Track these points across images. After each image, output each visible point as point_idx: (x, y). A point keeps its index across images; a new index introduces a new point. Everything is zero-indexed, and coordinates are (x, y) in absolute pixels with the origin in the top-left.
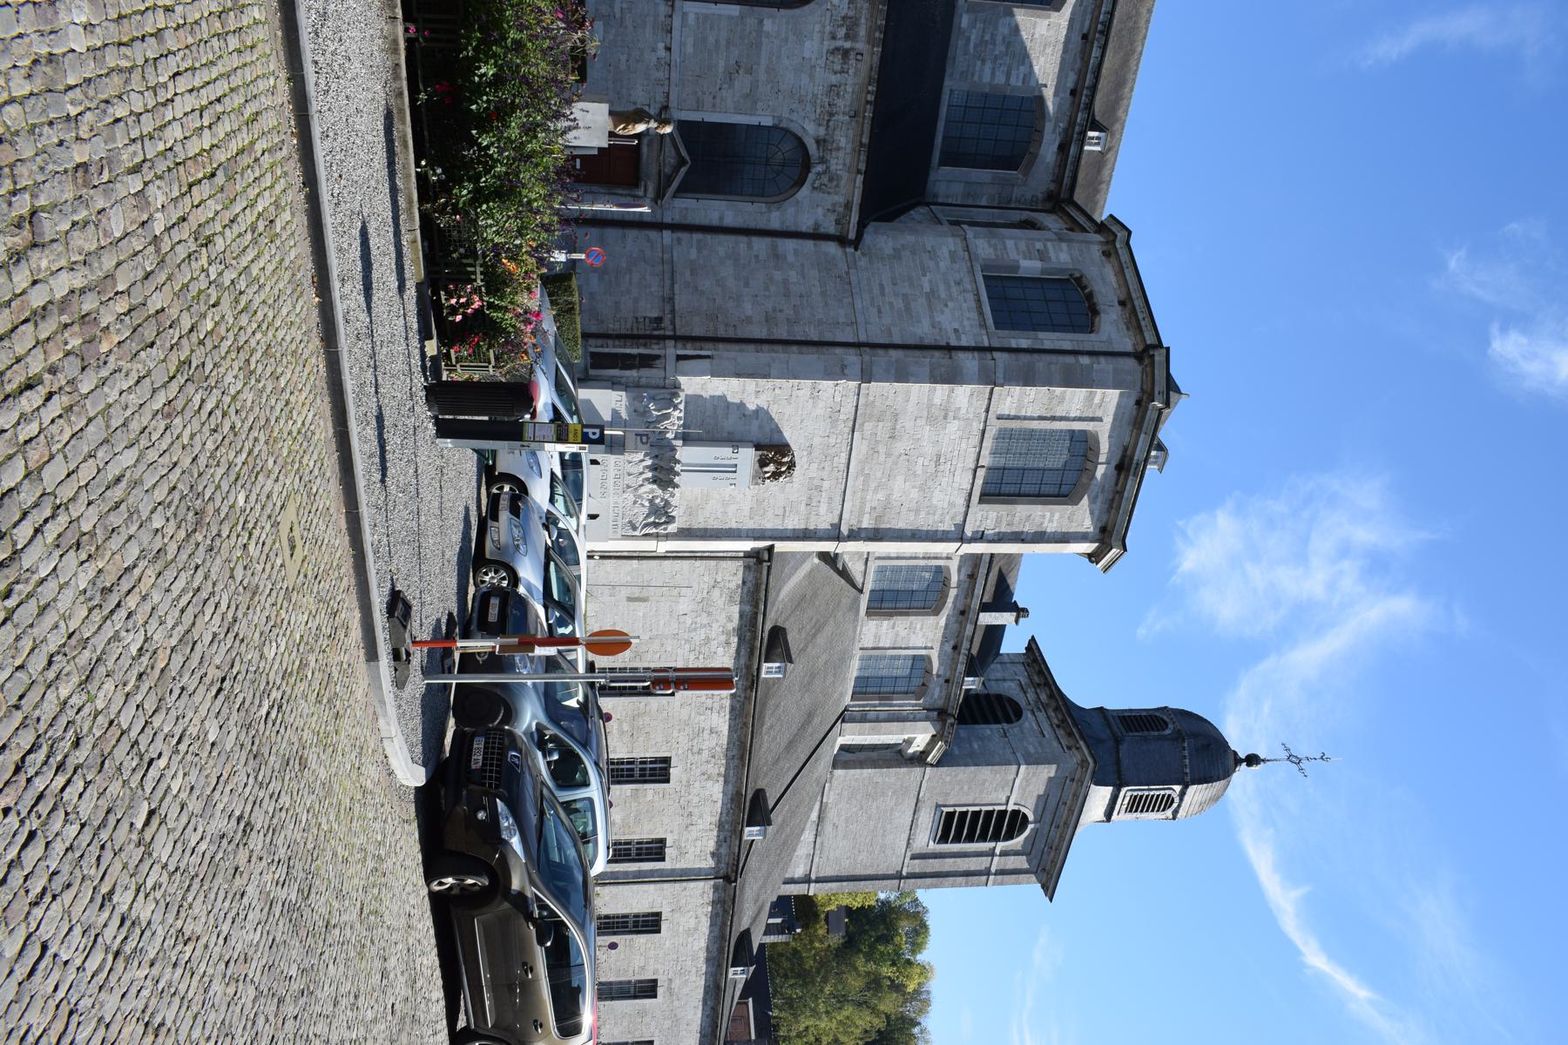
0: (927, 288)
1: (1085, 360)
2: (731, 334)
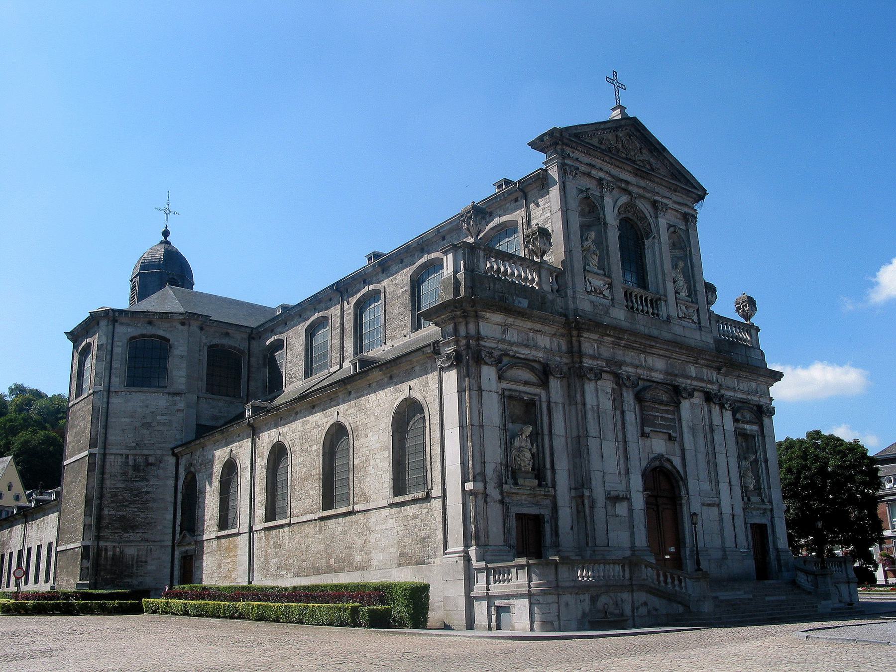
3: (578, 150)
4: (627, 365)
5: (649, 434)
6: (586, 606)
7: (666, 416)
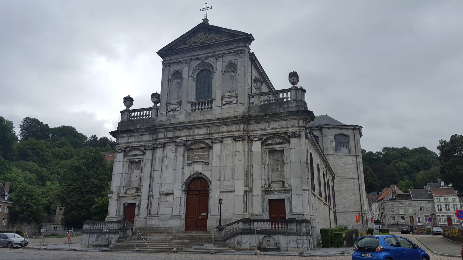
0: (343, 164)
1: (356, 139)
2: (359, 201)
4: (180, 137)
6: (94, 239)
7: (202, 153)
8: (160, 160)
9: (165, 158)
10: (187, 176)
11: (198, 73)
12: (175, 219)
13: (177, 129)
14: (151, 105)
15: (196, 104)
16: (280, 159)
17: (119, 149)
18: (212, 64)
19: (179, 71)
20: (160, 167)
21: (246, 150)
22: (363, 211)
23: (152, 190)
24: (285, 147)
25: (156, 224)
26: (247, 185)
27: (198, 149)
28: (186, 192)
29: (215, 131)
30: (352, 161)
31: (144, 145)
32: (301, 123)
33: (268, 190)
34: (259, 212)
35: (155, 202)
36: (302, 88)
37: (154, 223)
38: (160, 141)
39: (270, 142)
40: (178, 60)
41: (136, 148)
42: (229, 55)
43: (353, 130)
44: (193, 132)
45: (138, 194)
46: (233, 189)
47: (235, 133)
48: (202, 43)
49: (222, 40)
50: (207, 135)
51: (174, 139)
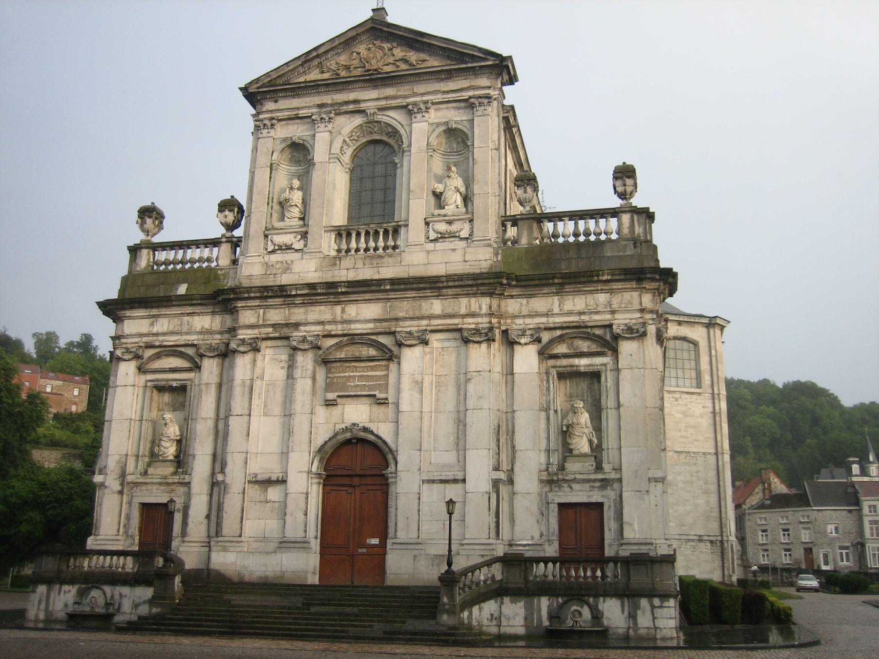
0: (681, 416)
1: (713, 352)
2: (717, 510)
3: (280, 97)
4: (306, 324)
5: (335, 400)
7: (370, 373)
8: (244, 386)
9: (257, 383)
10: (322, 436)
11: (355, 150)
12: (292, 550)
13: (297, 302)
14: (217, 231)
15: (349, 235)
16: (587, 397)
17: (124, 350)
18: (399, 129)
19: (301, 142)
20: (246, 405)
21: (498, 368)
22: (724, 534)
23: (222, 469)
24: (605, 365)
25: (238, 563)
26: (499, 465)
27: (358, 360)
28: (320, 478)
29: (407, 312)
30: (703, 407)
31: (195, 342)
32: (647, 300)
33: (558, 479)
34: (533, 538)
35: (232, 503)
36: (648, 208)
37: (233, 560)
38: (243, 334)
39: (562, 349)
40: (301, 112)
41: (173, 351)
42: (447, 108)
43: (707, 327)
44: (343, 311)
45: (181, 477)
46: (459, 473)
47: (464, 319)
48: (370, 70)
49: (426, 68)
50: (384, 324)
51: (286, 331)
